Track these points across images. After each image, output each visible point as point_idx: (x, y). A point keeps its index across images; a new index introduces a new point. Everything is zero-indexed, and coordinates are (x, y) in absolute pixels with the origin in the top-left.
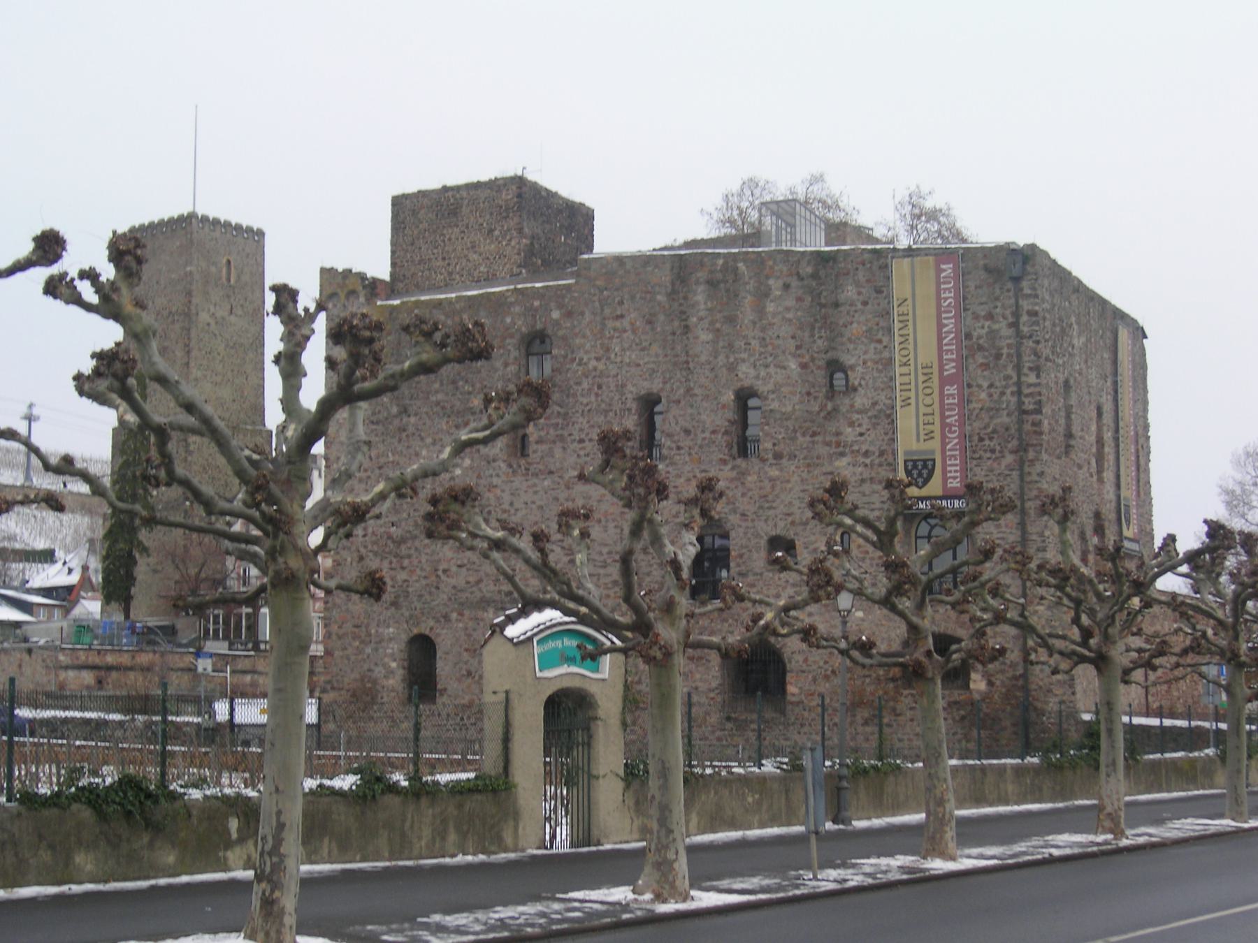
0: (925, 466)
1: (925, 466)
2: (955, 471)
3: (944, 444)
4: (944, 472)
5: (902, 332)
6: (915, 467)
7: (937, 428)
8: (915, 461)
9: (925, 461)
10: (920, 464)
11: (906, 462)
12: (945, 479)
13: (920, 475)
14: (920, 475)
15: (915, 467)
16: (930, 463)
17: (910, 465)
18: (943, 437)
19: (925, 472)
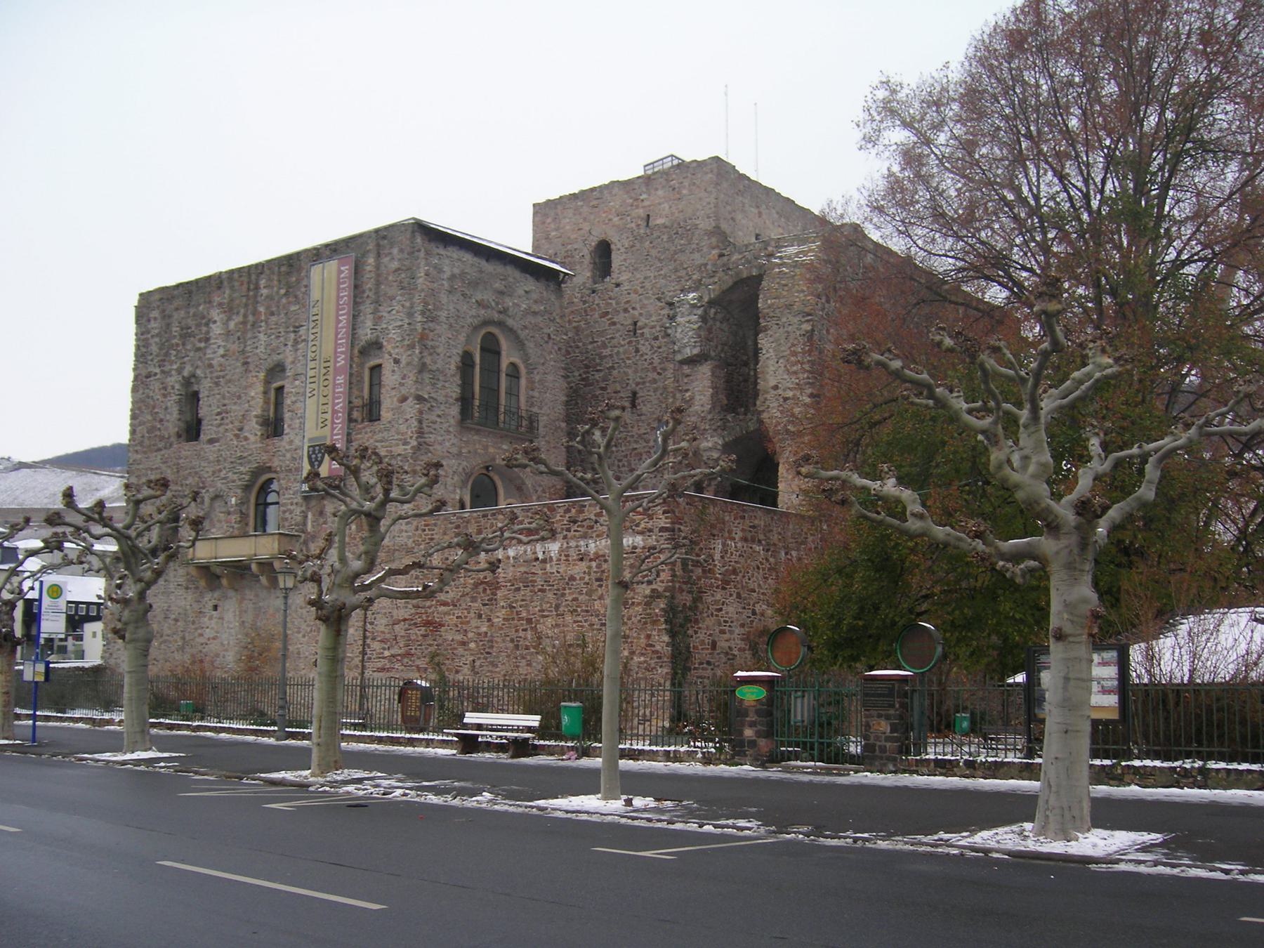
7: (328, 416)
13: (316, 460)
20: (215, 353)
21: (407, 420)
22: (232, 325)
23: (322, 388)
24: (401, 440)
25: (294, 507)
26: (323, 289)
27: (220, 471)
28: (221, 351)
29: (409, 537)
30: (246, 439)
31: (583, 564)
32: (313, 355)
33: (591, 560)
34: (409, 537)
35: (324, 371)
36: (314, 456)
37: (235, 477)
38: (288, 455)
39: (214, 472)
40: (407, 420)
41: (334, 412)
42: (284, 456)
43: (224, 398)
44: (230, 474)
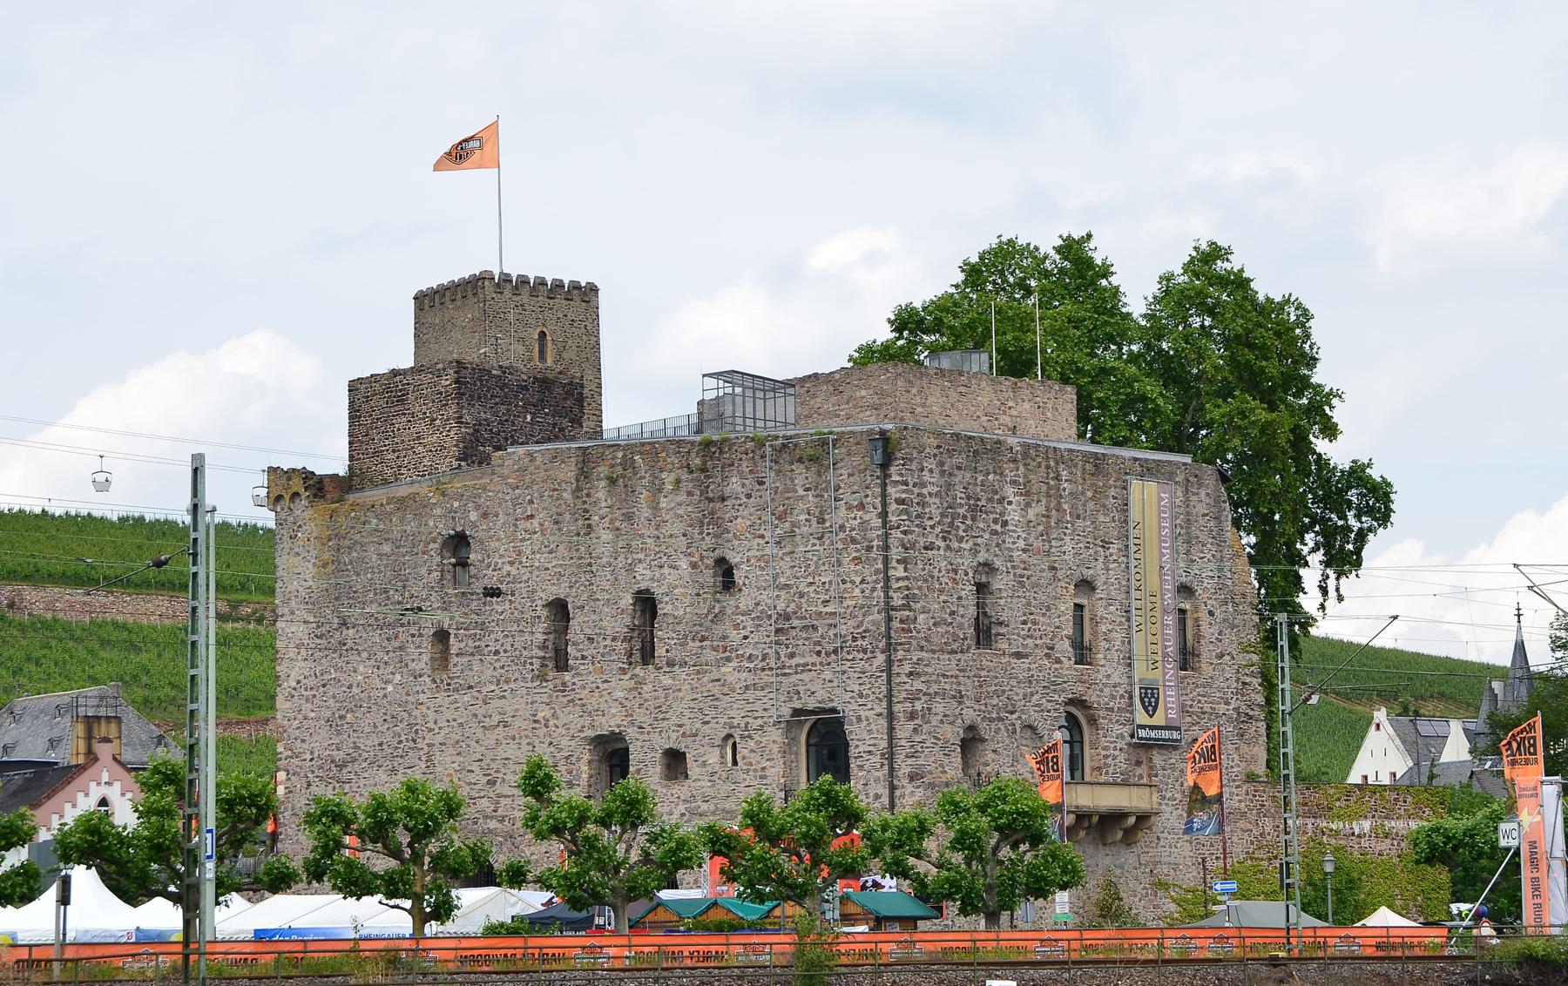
0: (1152, 694)
1: (1152, 694)
2: (1173, 702)
3: (1165, 674)
4: (1166, 702)
5: (1137, 556)
6: (1146, 694)
7: (1159, 658)
8: (1146, 689)
9: (1153, 689)
10: (1149, 691)
11: (1141, 688)
12: (1166, 709)
13: (1150, 703)
14: (1150, 703)
15: (1146, 694)
16: (1155, 691)
17: (1143, 691)
18: (1164, 667)
19: (1153, 700)
20: (1014, 543)
21: (1227, 679)
22: (1031, 514)
23: (1149, 625)
24: (1222, 698)
25: (1117, 753)
26: (1144, 512)
27: (1032, 694)
28: (1021, 544)
29: (1240, 801)
30: (1058, 661)
31: (1388, 841)
32: (1138, 584)
33: (1393, 839)
34: (1240, 801)
35: (1150, 606)
36: (1146, 700)
37: (1049, 706)
38: (1107, 690)
39: (1025, 696)
40: (1227, 679)
41: (1165, 655)
42: (1101, 690)
43: (1029, 604)
44: (1044, 700)
